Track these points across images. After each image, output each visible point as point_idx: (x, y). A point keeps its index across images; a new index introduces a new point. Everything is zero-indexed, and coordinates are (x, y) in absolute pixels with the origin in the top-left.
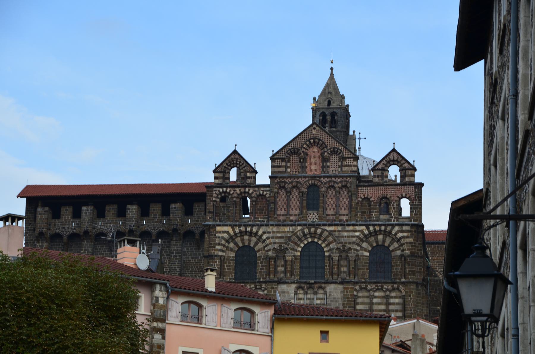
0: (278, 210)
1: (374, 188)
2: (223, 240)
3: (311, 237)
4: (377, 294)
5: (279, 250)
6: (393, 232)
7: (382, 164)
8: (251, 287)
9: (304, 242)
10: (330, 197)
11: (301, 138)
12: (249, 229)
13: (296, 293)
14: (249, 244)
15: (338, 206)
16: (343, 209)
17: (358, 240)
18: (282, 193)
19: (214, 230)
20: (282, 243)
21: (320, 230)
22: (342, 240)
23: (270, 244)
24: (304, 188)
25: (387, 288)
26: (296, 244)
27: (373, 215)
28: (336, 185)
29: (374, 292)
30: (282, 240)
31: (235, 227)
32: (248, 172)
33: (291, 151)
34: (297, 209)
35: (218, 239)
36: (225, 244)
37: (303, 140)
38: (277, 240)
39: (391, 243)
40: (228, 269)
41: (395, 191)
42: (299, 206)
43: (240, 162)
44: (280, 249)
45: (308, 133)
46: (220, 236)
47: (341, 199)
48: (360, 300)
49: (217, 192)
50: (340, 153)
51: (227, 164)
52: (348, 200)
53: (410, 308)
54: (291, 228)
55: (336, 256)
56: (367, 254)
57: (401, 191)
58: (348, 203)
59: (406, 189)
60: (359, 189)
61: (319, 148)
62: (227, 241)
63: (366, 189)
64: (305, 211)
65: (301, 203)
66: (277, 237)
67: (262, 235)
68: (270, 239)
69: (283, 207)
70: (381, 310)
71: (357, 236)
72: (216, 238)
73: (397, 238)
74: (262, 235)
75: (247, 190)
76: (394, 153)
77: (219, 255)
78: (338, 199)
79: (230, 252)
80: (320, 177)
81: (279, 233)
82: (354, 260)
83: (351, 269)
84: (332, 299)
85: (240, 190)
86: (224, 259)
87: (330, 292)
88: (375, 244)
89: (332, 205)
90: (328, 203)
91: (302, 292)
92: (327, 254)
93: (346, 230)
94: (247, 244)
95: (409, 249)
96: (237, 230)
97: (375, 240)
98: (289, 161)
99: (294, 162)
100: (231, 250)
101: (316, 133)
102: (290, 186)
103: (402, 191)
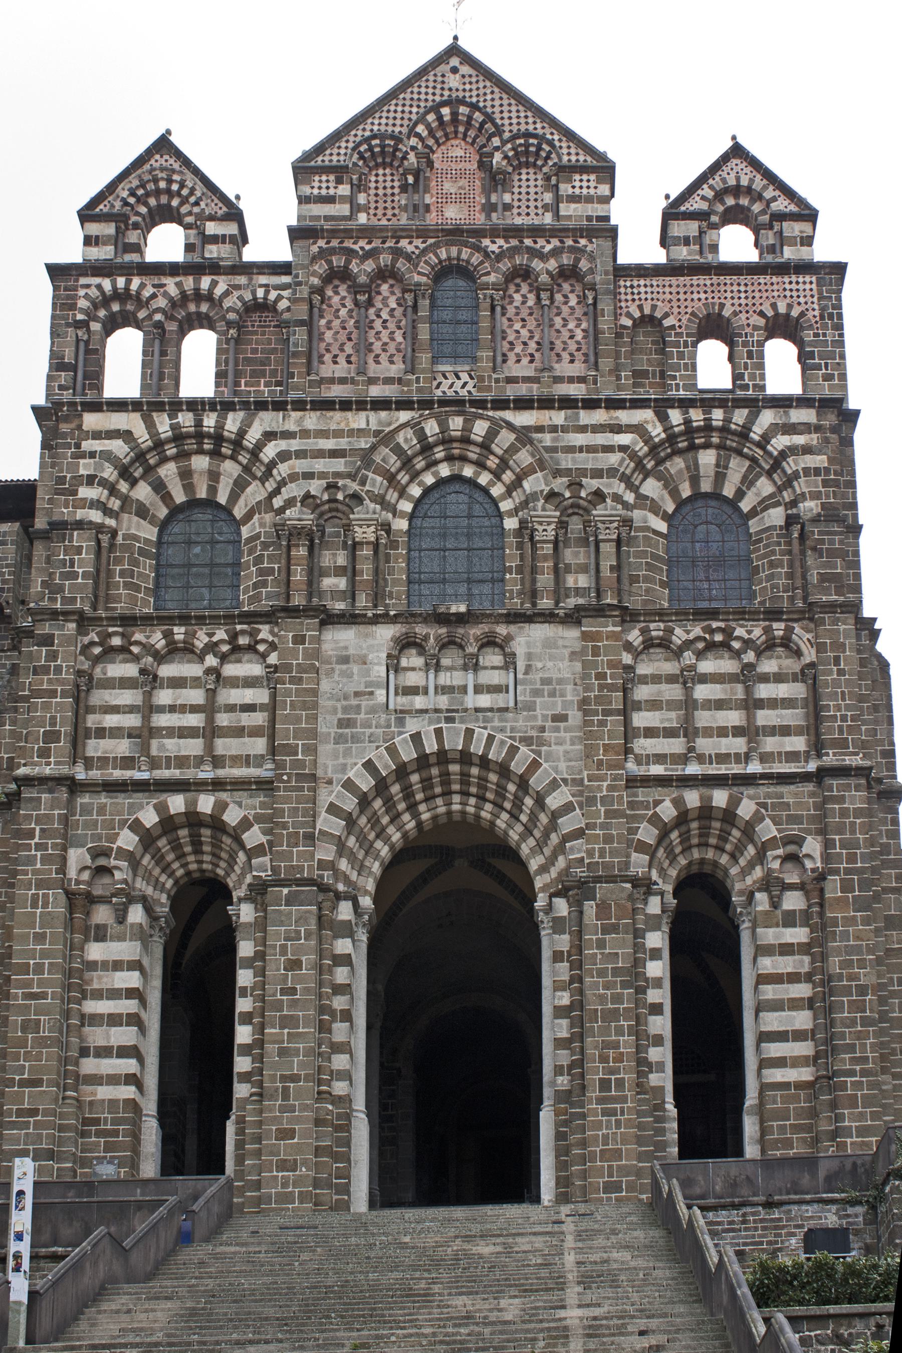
0: (323, 363)
1: (674, 280)
2: (107, 464)
4: (707, 666)
7: (697, 199)
10: (517, 314)
11: (408, 103)
12: (210, 421)
13: (394, 665)
15: (546, 345)
16: (566, 356)
17: (628, 461)
19: (73, 426)
20: (337, 475)
22: (566, 461)
23: (293, 477)
24: (419, 273)
26: (391, 478)
28: (537, 265)
29: (700, 655)
30: (339, 465)
31: (154, 414)
32: (212, 218)
33: (371, 149)
34: (395, 359)
35: (87, 461)
37: (415, 110)
38: (319, 465)
42: (403, 346)
43: (182, 185)
46: (99, 449)
47: (558, 321)
48: (642, 693)
49: (94, 292)
50: (548, 157)
51: (132, 193)
52: (584, 325)
54: (372, 416)
55: (549, 524)
58: (584, 338)
59: (788, 286)
60: (622, 283)
63: (645, 286)
65: (412, 335)
66: (320, 454)
67: (259, 446)
71: (623, 448)
72: (83, 455)
73: (770, 454)
74: (259, 446)
75: (205, 282)
76: (738, 161)
77: (91, 522)
78: (545, 323)
80: (479, 233)
82: (615, 537)
83: (606, 572)
84: (538, 686)
85: (179, 285)
89: (525, 344)
90: (511, 337)
91: (419, 661)
98: (359, 186)
99: (381, 192)
101: (461, 87)
102: (369, 266)
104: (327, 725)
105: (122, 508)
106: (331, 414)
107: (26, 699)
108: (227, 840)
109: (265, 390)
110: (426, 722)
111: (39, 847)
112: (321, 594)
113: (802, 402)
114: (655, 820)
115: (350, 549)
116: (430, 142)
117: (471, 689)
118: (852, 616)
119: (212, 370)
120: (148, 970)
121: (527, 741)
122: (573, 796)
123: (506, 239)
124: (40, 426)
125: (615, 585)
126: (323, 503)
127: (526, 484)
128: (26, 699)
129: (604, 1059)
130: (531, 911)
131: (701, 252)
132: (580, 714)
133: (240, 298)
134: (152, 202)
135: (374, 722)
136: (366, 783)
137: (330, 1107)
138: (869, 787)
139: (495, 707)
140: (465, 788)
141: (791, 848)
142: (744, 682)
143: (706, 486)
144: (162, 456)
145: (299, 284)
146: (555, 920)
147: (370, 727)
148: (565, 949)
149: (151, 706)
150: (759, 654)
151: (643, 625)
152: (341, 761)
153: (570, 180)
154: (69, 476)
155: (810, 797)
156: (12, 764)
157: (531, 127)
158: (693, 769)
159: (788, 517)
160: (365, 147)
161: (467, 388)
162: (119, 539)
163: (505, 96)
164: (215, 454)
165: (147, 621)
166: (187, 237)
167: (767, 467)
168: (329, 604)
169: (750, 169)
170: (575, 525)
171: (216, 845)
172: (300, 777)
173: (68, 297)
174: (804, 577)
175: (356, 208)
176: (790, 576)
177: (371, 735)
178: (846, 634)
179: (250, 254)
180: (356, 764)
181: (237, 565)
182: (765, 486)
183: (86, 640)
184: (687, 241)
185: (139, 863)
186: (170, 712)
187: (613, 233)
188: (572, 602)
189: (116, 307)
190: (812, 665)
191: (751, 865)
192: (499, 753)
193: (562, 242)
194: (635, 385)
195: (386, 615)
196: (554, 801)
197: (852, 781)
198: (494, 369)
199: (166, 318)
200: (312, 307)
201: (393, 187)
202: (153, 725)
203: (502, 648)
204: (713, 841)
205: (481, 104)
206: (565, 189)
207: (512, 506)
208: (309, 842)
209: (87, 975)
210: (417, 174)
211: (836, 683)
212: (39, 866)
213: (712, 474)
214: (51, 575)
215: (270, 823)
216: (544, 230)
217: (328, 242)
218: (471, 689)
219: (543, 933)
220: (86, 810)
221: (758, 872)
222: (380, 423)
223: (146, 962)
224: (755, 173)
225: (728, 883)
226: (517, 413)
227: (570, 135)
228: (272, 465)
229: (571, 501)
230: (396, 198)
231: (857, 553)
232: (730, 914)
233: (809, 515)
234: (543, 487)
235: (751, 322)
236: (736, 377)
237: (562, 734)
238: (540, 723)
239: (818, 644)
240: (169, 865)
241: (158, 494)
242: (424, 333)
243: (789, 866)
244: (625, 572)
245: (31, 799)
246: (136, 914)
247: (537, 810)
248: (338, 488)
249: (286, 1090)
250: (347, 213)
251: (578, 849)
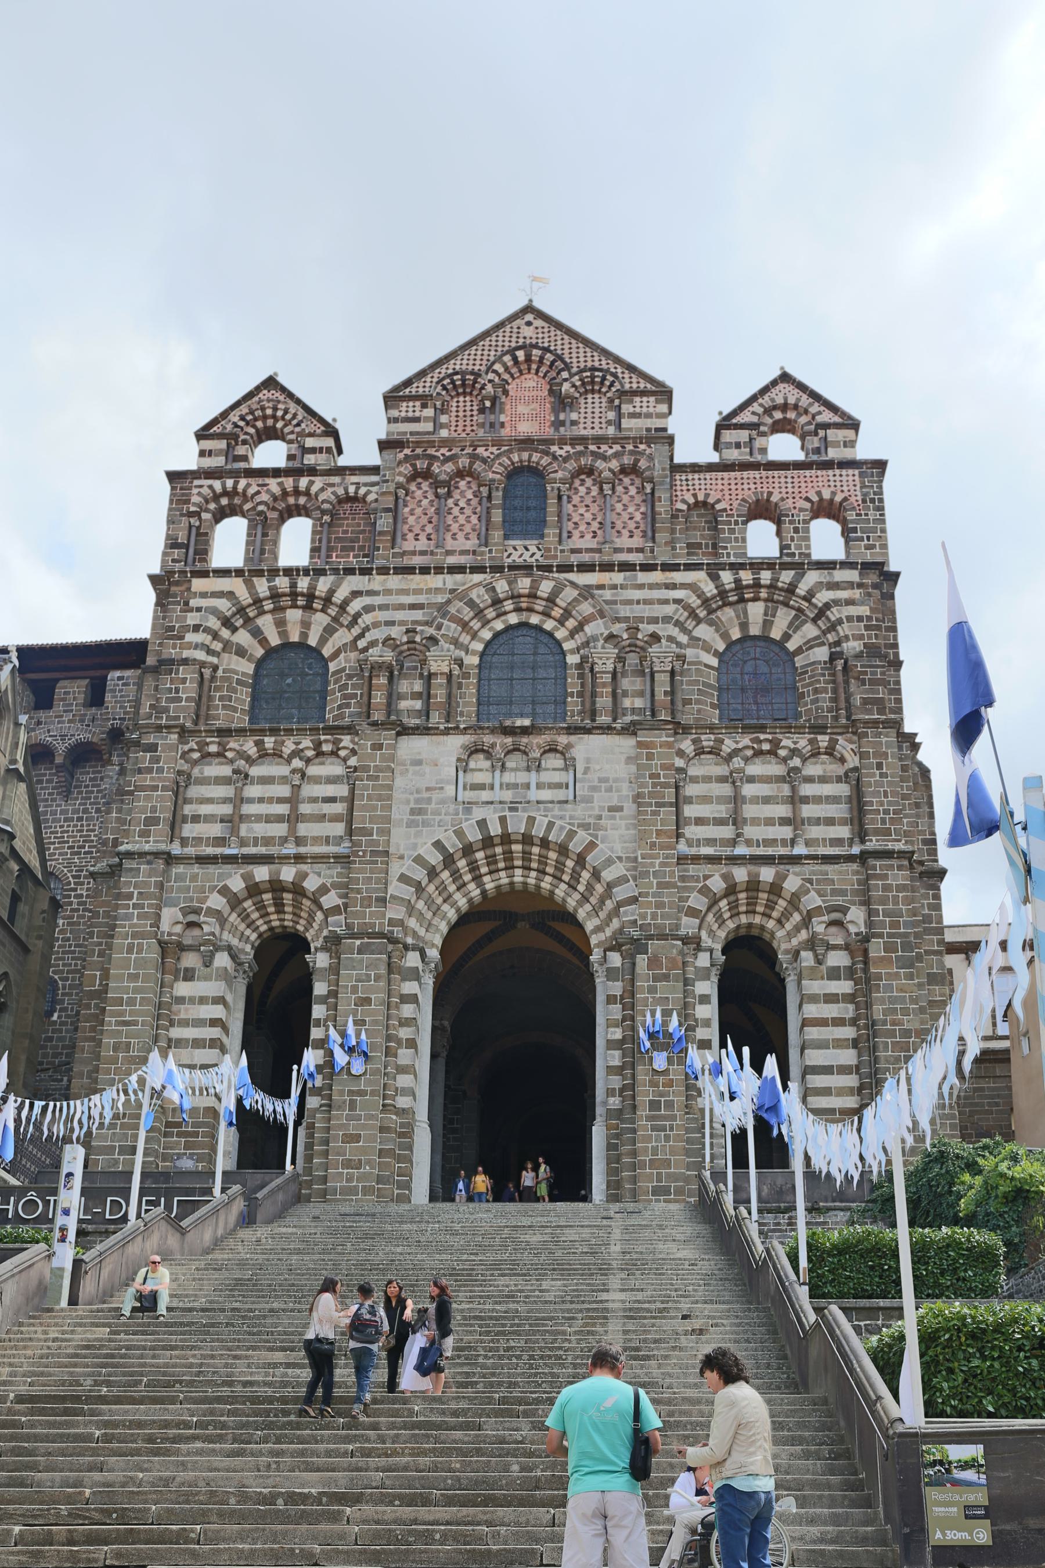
1: (726, 475)
2: (211, 616)
3: (518, 610)
4: (755, 769)
5: (406, 647)
6: (802, 589)
7: (749, 414)
8: (301, 747)
9: (492, 624)
11: (487, 348)
12: (303, 584)
13: (463, 766)
14: (304, 635)
15: (608, 525)
18: (422, 491)
19: (183, 588)
21: (552, 584)
22: (624, 611)
23: (376, 625)
24: (494, 472)
25: (792, 746)
26: (465, 625)
27: (726, 548)
28: (600, 464)
29: (747, 760)
30: (418, 615)
31: (255, 579)
32: (311, 435)
33: (453, 382)
35: (194, 614)
36: (220, 629)
37: (493, 353)
38: (399, 615)
39: (795, 625)
40: (224, 707)
41: (796, 485)
42: (478, 527)
43: (286, 411)
44: (408, 642)
45: (508, 334)
47: (619, 507)
49: (205, 491)
50: (612, 385)
51: (242, 418)
53: (882, 804)
54: (449, 578)
56: (714, 662)
57: (815, 484)
59: (832, 478)
60: (678, 477)
61: (544, 377)
62: (227, 623)
64: (497, 535)
66: (401, 607)
67: (346, 602)
68: (377, 613)
69: (423, 530)
72: (191, 610)
73: (815, 606)
74: (346, 602)
75: (304, 482)
76: (786, 385)
77: (195, 660)
79: (236, 657)
80: (549, 442)
81: (408, 595)
82: (669, 668)
83: (660, 696)
84: (596, 783)
85: (280, 484)
86: (213, 678)
87: (588, 760)
88: (736, 634)
89: (588, 524)
90: (576, 518)
92: (572, 659)
93: (639, 582)
94: (295, 638)
95: (861, 637)
96: (262, 587)
97: (738, 617)
99: (461, 414)
100: (241, 652)
101: (535, 336)
102: (449, 467)
103: (820, 484)
104: (399, 812)
105: (224, 650)
106: (412, 576)
107: (131, 793)
108: (306, 903)
109: (352, 560)
110: (491, 810)
112: (398, 712)
113: (845, 565)
114: (705, 891)
115: (426, 679)
116: (506, 376)
117: (533, 786)
118: (894, 731)
119: (308, 546)
120: (231, 1004)
121: (586, 827)
122: (627, 870)
123: (572, 445)
124: (155, 589)
125: (669, 706)
126: (402, 644)
127: (586, 628)
128: (131, 793)
129: (654, 1084)
130: (587, 963)
131: (751, 454)
132: (635, 806)
133: (334, 493)
134: (260, 424)
135: (443, 811)
136: (435, 858)
137: (394, 1117)
138: (911, 867)
139: (556, 800)
140: (526, 864)
141: (835, 916)
142: (790, 783)
143: (755, 630)
144: (260, 610)
145: (387, 481)
146: (608, 970)
147: (440, 814)
148: (618, 994)
149: (242, 799)
150: (804, 760)
151: (694, 736)
152: (413, 840)
153: (632, 402)
154: (177, 625)
155: (853, 875)
156: (116, 843)
157: (597, 364)
158: (741, 850)
159: (832, 654)
160: (448, 381)
161: (535, 557)
162: (220, 673)
163: (573, 341)
164: (308, 607)
165: (241, 732)
166: (289, 450)
167: (812, 616)
168: (405, 720)
169: (797, 390)
170: (632, 659)
171: (297, 906)
172: (374, 853)
173: (183, 495)
174: (847, 700)
175: (437, 426)
176: (835, 700)
177: (441, 820)
178: (888, 745)
179: (342, 461)
181: (324, 694)
182: (810, 631)
183: (186, 748)
184: (738, 445)
185: (226, 920)
186: (259, 802)
187: (670, 440)
188: (628, 719)
189: (224, 501)
190: (856, 769)
191: (797, 929)
192: (558, 836)
193: (623, 447)
194: (688, 554)
195: (457, 728)
196: (608, 875)
197: (895, 862)
198: (560, 542)
199: (268, 508)
200: (397, 498)
201: (472, 410)
202: (242, 812)
203: (562, 753)
204: (760, 909)
205: (552, 348)
206: (626, 408)
207: (575, 646)
208: (380, 904)
209: (175, 1007)
210: (494, 400)
211: (878, 784)
212: (135, 921)
213: (761, 621)
214: (158, 700)
215: (345, 888)
216: (608, 439)
217: (413, 451)
218: (533, 786)
219: (597, 981)
220: (180, 878)
221: (804, 935)
222: (455, 583)
223: (229, 998)
224: (801, 393)
225: (775, 944)
226: (580, 575)
227: (631, 368)
228: (357, 616)
229: (628, 642)
230: (475, 418)
231: (898, 683)
232: (777, 969)
233: (852, 652)
234: (603, 630)
235: (797, 505)
236: (782, 548)
237: (618, 821)
238: (597, 812)
239: (861, 753)
240: (254, 922)
241: (255, 638)
242: (497, 516)
243: (833, 930)
244: (679, 696)
245: (131, 869)
246: (222, 960)
247: (593, 881)
248: (416, 632)
249: (353, 1103)
250: (431, 429)
251: (629, 913)
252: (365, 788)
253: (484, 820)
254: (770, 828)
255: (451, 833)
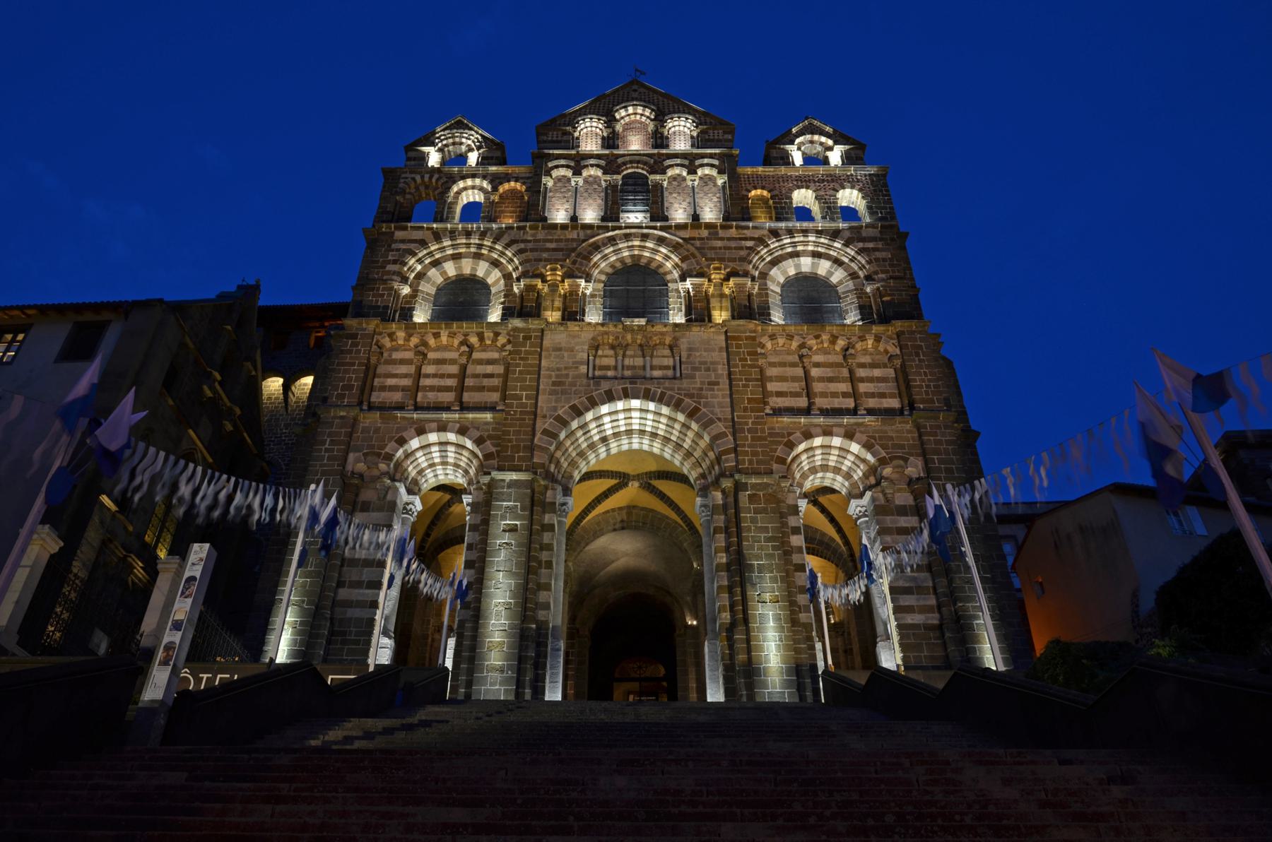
70: (838, 393)
72: (393, 251)
84: (697, 365)
87: (690, 349)
95: (887, 272)
111: (326, 450)
122: (726, 428)
147: (575, 386)
152: (553, 404)
180: (563, 407)
212: (325, 461)
237: (716, 392)
238: (698, 386)
252: (517, 366)
253: (610, 391)
254: (836, 400)
255: (584, 399)
